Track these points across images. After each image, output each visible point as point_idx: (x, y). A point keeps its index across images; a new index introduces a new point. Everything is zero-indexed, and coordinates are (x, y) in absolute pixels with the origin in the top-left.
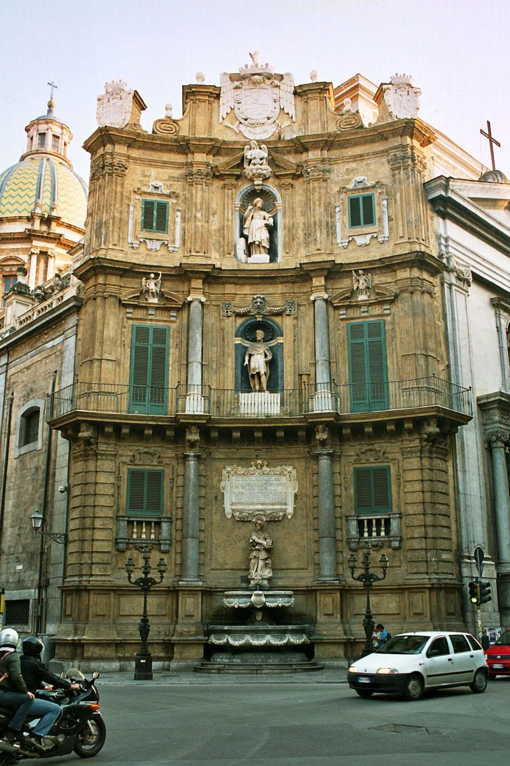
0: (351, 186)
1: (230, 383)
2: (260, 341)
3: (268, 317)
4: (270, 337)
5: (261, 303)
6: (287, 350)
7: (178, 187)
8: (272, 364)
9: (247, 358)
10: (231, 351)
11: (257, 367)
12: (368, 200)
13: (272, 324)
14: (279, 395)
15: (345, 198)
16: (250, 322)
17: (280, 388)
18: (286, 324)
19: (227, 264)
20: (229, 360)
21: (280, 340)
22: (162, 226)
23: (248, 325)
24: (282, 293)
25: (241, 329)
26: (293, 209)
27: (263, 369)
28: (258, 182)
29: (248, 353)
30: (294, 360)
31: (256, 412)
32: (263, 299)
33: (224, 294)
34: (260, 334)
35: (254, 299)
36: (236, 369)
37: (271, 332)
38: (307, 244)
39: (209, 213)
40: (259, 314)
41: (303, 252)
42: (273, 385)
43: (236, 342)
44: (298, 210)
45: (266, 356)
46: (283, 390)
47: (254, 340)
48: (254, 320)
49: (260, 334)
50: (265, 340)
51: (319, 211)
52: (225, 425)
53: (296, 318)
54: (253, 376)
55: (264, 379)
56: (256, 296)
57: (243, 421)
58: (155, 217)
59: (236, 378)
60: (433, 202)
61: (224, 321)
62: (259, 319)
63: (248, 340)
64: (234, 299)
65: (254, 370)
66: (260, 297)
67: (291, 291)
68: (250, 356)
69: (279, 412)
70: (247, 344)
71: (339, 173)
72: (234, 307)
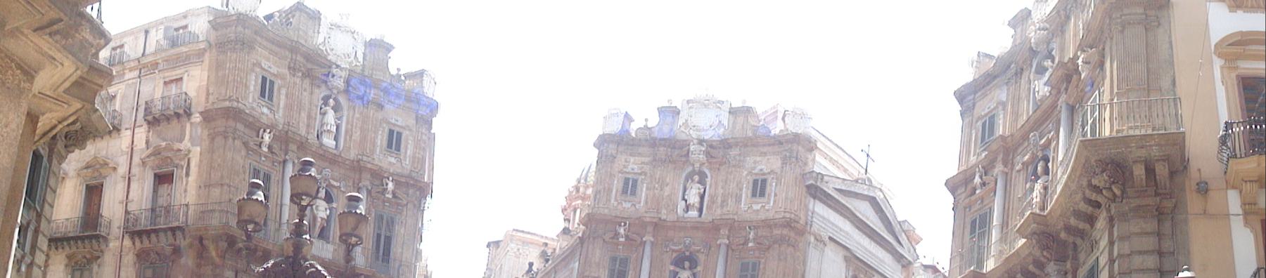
0: (756, 171)
7: (647, 168)
12: (764, 181)
15: (751, 179)
19: (671, 218)
22: (634, 193)
26: (716, 183)
28: (697, 165)
38: (722, 207)
39: (663, 184)
41: (719, 211)
44: (721, 184)
51: (733, 186)
58: (630, 187)
60: (808, 187)
71: (750, 161)
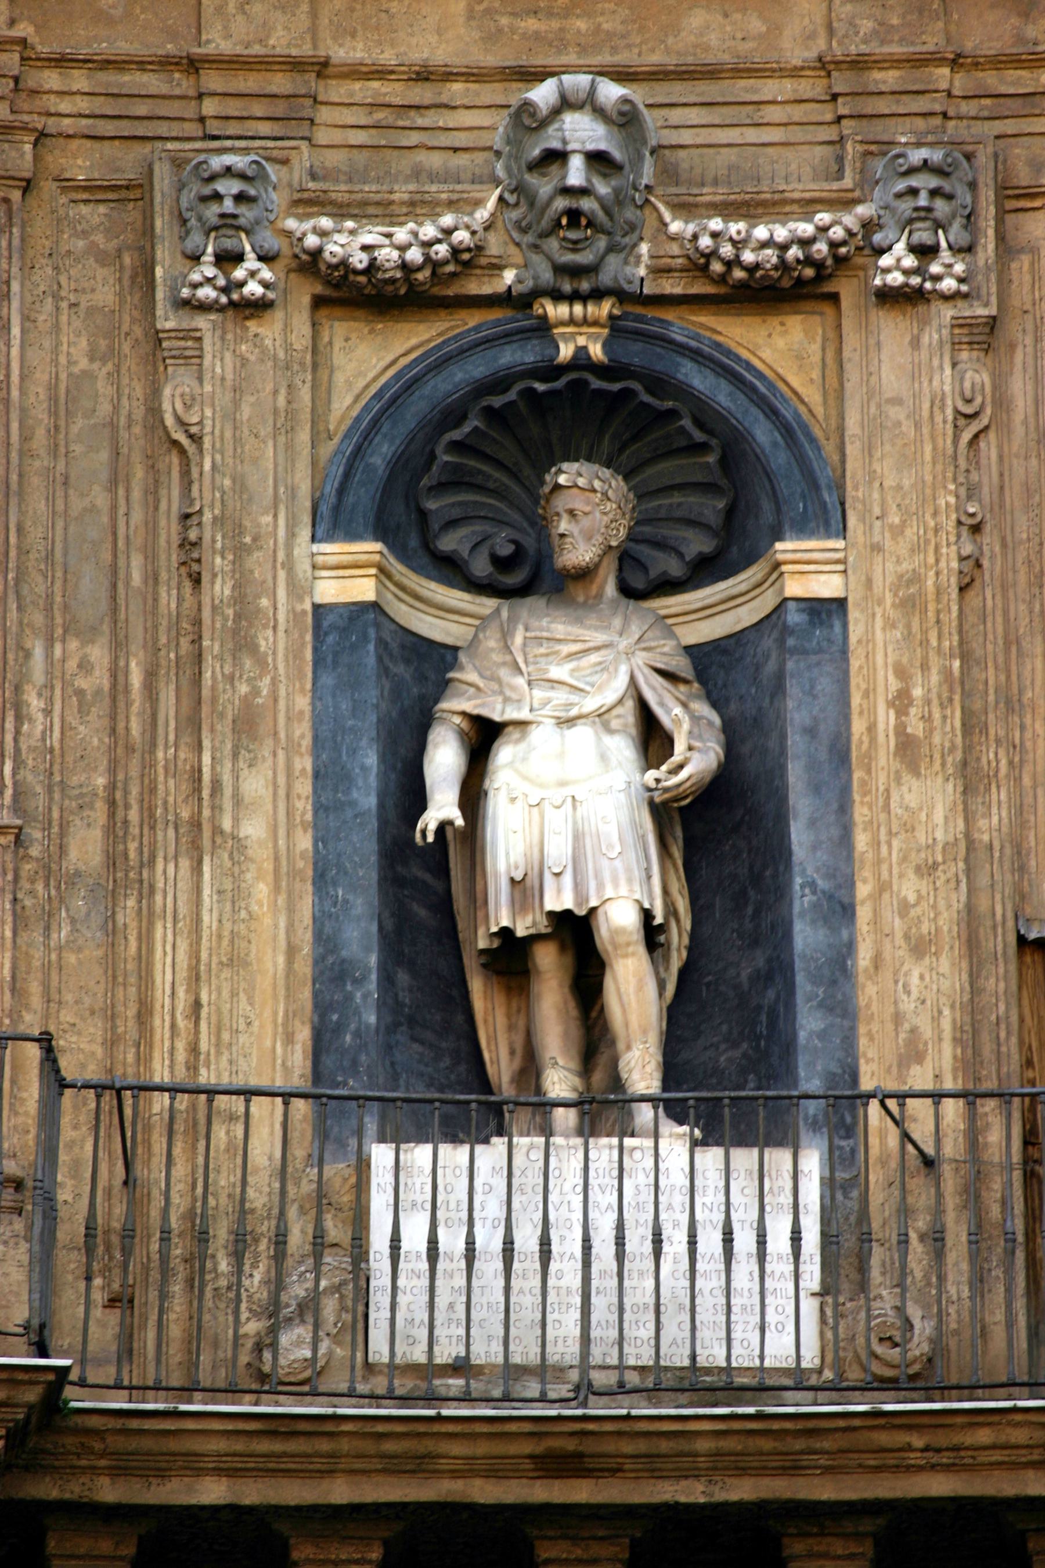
1: (264, 1038)
2: (584, 574)
3: (681, 324)
4: (697, 544)
5: (597, 159)
6: (887, 679)
8: (722, 833)
9: (444, 759)
10: (285, 685)
11: (558, 851)
13: (722, 396)
14: (812, 1163)
16: (476, 369)
17: (810, 1081)
18: (878, 394)
20: (255, 784)
21: (807, 568)
23: (451, 415)
24: (824, 65)
25: (381, 455)
27: (624, 888)
29: (457, 704)
30: (971, 781)
31: (564, 1343)
32: (625, 120)
33: (193, 65)
34: (588, 507)
35: (527, 121)
36: (324, 875)
37: (714, 483)
40: (577, 283)
42: (739, 1055)
43: (331, 590)
45: (653, 739)
46: (845, 1104)
47: (526, 575)
48: (512, 356)
49: (588, 507)
50: (642, 577)
52: (213, 1492)
53: (985, 336)
54: (511, 957)
55: (635, 993)
56: (543, 94)
57: (412, 1445)
59: (331, 974)
61: (193, 359)
62: (579, 335)
63: (450, 569)
64: (296, 117)
65: (525, 890)
66: (589, 103)
67: (932, 41)
68: (483, 737)
69: (810, 1358)
70: (441, 612)
72: (307, 203)
